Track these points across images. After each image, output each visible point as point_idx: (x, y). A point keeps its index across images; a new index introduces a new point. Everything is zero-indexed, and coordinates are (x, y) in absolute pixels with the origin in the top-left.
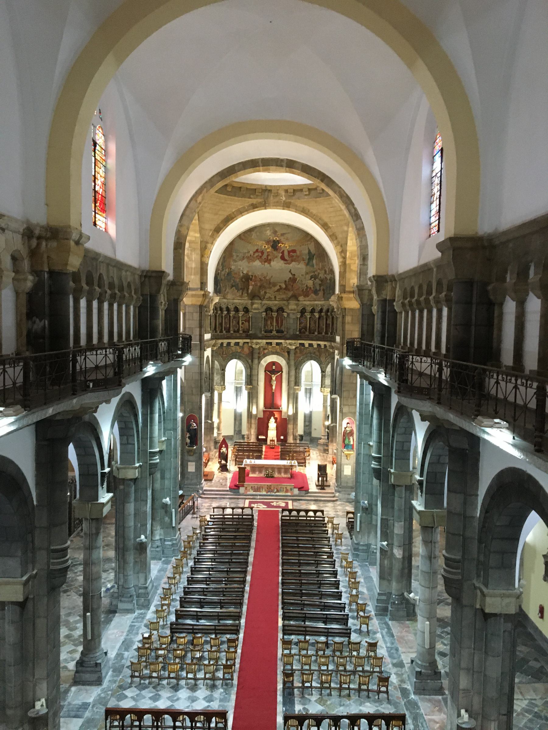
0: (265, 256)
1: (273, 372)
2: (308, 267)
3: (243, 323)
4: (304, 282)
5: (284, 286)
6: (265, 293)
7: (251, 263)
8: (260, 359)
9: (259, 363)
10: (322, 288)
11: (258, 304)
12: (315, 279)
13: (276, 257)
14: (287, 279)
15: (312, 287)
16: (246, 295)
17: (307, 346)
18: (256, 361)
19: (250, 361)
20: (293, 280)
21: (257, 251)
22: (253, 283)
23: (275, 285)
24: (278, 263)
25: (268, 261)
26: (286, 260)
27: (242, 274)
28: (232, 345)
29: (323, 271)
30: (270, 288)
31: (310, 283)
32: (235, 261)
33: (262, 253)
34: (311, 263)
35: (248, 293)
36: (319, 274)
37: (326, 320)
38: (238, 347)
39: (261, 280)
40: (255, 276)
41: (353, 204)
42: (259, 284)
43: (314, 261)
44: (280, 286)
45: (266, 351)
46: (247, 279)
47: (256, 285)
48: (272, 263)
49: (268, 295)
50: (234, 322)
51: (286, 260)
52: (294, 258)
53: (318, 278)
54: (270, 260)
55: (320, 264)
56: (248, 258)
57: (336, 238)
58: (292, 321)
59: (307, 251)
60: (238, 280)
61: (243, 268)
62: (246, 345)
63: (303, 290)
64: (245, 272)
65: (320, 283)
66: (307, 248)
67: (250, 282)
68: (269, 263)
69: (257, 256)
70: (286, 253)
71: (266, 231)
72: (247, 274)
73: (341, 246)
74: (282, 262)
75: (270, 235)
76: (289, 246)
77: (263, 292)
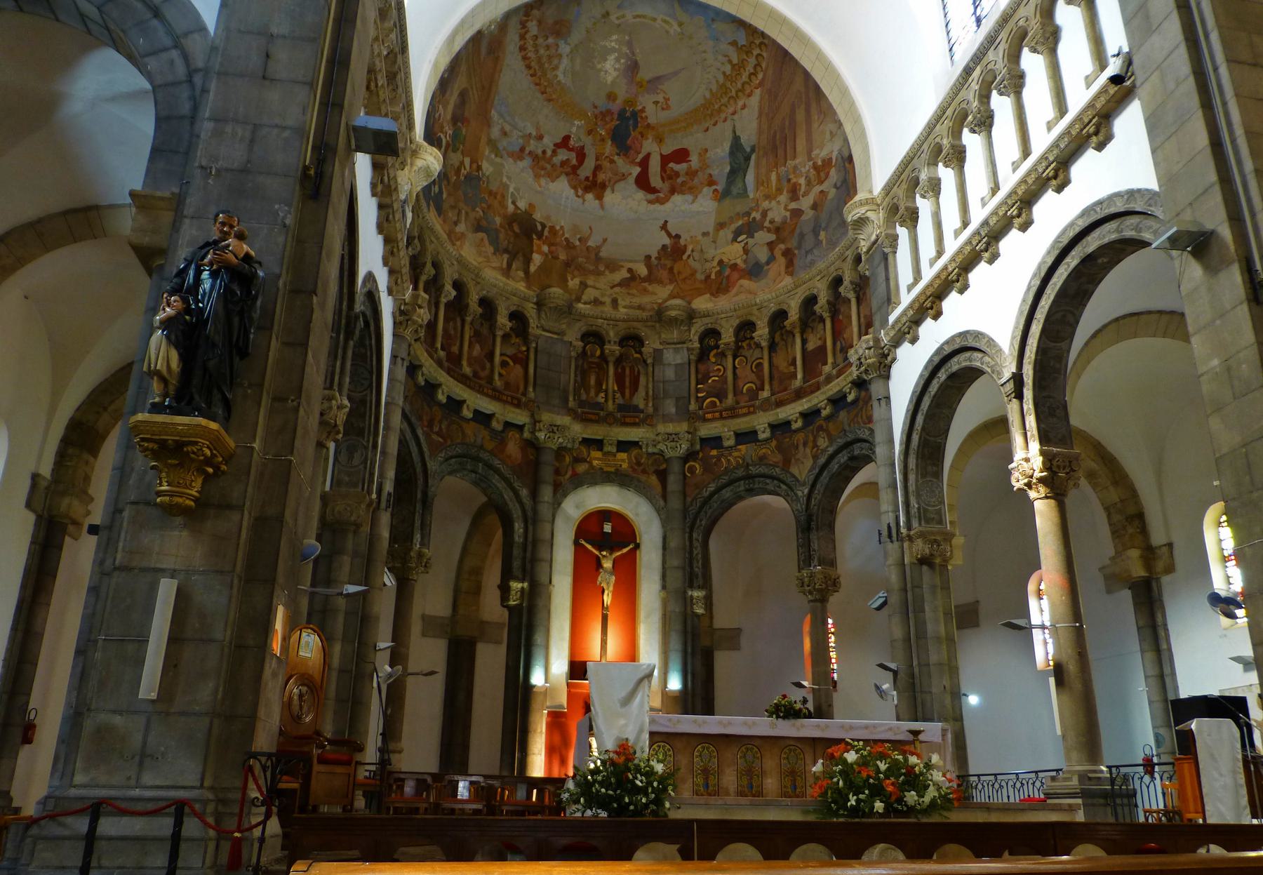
0: (586, 170)
1: (607, 543)
2: (727, 201)
3: (504, 364)
4: (711, 252)
5: (642, 270)
6: (584, 285)
7: (543, 181)
8: (560, 491)
9: (557, 504)
10: (778, 252)
13: (623, 177)
15: (739, 261)
16: (521, 274)
18: (547, 493)
19: (524, 492)
20: (675, 251)
21: (565, 143)
22: (545, 248)
23: (613, 266)
27: (511, 208)
28: (467, 413)
29: (783, 198)
30: (599, 274)
31: (733, 252)
33: (581, 156)
35: (527, 272)
36: (764, 214)
37: (804, 342)
38: (484, 433)
39: (569, 246)
40: (552, 228)
42: (563, 256)
43: (750, 178)
44: (630, 270)
45: (582, 468)
47: (556, 258)
48: (609, 197)
49: (590, 294)
50: (477, 347)
52: (679, 180)
53: (762, 228)
54: (603, 187)
55: (773, 177)
56: (536, 158)
58: (670, 374)
59: (727, 146)
60: (498, 220)
61: (517, 189)
62: (513, 435)
63: (708, 277)
64: (522, 205)
65: (772, 237)
67: (536, 242)
68: (599, 197)
69: (563, 163)
70: (655, 165)
74: (641, 195)
77: (577, 281)
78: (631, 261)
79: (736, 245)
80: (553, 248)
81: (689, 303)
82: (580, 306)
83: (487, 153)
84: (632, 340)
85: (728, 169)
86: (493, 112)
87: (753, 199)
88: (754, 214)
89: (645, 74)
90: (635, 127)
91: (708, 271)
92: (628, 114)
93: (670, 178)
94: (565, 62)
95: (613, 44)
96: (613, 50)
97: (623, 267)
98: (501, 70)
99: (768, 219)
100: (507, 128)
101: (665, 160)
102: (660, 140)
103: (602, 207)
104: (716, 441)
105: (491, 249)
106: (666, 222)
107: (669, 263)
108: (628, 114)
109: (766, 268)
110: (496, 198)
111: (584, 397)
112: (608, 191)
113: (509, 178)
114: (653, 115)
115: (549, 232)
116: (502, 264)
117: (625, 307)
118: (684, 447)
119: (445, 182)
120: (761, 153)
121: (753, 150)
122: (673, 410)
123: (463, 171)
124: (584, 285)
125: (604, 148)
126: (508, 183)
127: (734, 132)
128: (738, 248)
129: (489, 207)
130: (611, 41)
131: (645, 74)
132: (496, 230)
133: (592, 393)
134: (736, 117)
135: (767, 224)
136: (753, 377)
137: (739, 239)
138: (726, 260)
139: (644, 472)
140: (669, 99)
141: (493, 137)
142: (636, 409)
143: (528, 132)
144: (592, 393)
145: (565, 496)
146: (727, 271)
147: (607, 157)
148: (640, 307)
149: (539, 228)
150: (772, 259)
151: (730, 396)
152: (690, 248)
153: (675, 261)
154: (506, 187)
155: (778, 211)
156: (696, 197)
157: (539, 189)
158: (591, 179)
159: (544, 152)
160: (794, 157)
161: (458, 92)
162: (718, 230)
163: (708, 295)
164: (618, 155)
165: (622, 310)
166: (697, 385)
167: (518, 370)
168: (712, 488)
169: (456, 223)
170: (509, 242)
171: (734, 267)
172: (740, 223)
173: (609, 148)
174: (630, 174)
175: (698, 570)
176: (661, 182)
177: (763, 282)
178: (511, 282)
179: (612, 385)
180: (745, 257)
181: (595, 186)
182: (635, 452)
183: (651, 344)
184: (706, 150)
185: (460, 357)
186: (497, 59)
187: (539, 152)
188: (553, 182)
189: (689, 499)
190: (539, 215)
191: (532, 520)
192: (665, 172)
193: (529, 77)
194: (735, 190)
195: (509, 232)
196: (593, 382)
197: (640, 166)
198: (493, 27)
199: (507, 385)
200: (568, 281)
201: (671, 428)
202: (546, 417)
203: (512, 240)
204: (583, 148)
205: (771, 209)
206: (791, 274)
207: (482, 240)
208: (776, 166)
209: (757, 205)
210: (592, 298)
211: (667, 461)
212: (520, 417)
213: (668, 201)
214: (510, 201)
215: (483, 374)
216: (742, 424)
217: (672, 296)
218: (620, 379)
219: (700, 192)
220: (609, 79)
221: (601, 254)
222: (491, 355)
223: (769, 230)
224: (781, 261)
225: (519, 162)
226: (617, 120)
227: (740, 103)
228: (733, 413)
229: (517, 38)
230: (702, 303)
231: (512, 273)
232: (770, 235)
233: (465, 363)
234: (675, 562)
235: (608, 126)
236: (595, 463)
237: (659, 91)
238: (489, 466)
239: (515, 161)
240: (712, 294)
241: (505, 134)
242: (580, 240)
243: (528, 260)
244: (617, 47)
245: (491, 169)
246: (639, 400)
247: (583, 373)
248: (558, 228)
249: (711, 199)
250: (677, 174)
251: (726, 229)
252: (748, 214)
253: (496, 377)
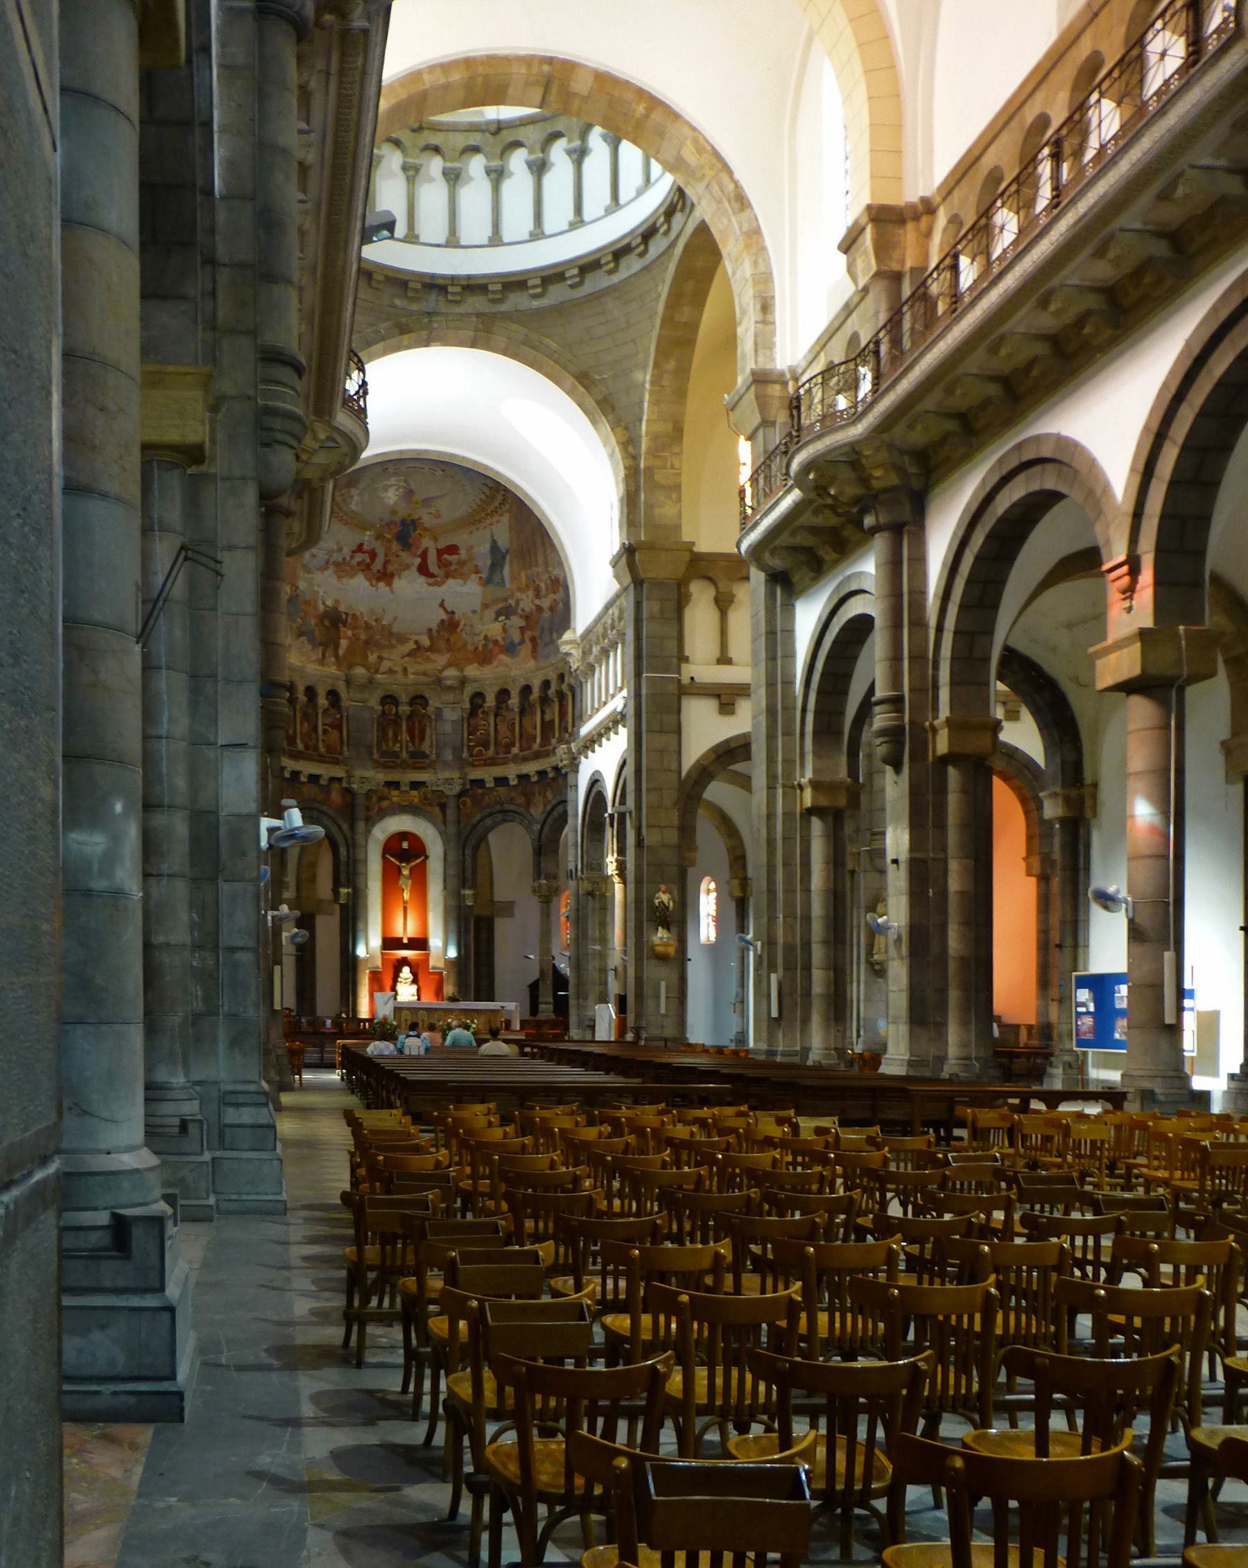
0: (378, 565)
1: (405, 856)
3: (325, 732)
5: (426, 642)
6: (381, 658)
7: (345, 580)
8: (370, 822)
9: (368, 832)
12: (508, 618)
13: (407, 567)
14: (434, 626)
15: (499, 638)
16: (333, 659)
17: (490, 784)
18: (361, 826)
19: (345, 826)
20: (450, 625)
21: (359, 549)
22: (350, 633)
23: (402, 639)
25: (385, 576)
26: (432, 576)
27: (321, 608)
29: (531, 593)
30: (392, 647)
31: (494, 629)
32: (307, 569)
33: (373, 555)
34: (496, 579)
35: (337, 656)
36: (518, 602)
37: (543, 713)
39: (368, 627)
41: (730, 172)
42: (363, 637)
43: (506, 571)
44: (416, 642)
45: (385, 804)
46: (335, 620)
47: (358, 639)
48: (397, 583)
49: (386, 665)
51: (432, 576)
52: (453, 568)
53: (515, 613)
54: (392, 575)
56: (337, 565)
57: (613, 409)
58: (448, 728)
59: (488, 546)
60: (313, 622)
62: (336, 786)
64: (329, 603)
65: (523, 623)
67: (342, 629)
68: (389, 584)
69: (359, 564)
71: (386, 488)
72: (335, 608)
73: (626, 429)
74: (422, 579)
81: (462, 670)
82: (379, 676)
84: (419, 700)
85: (489, 562)
88: (510, 601)
89: (419, 496)
94: (356, 498)
101: (440, 553)
102: (435, 539)
103: (392, 592)
104: (480, 783)
107: (446, 635)
111: (384, 748)
112: (396, 578)
114: (427, 520)
117: (414, 674)
118: (457, 789)
122: (450, 757)
124: (381, 658)
131: (419, 496)
133: (391, 743)
136: (508, 734)
139: (430, 804)
142: (424, 756)
144: (391, 743)
145: (374, 825)
146: (491, 646)
148: (424, 674)
149: (344, 616)
150: (522, 642)
151: (492, 748)
152: (462, 623)
154: (317, 593)
155: (527, 602)
165: (411, 677)
166: (469, 734)
167: (334, 734)
168: (478, 817)
171: (496, 642)
172: (500, 606)
173: (395, 546)
175: (469, 875)
178: (326, 669)
179: (405, 736)
181: (385, 576)
182: (423, 790)
183: (434, 703)
185: (295, 736)
187: (340, 559)
189: (462, 825)
191: (352, 845)
196: (391, 734)
199: (329, 748)
201: (447, 775)
202: (358, 773)
206: (535, 658)
211: (447, 796)
212: (338, 772)
215: (311, 744)
216: (498, 771)
217: (450, 665)
218: (411, 731)
222: (315, 728)
224: (528, 645)
228: (492, 762)
230: (472, 671)
233: (298, 741)
234: (451, 872)
236: (395, 799)
238: (320, 811)
240: (480, 664)
243: (337, 646)
246: (426, 747)
247: (383, 729)
250: (450, 563)
253: (321, 744)
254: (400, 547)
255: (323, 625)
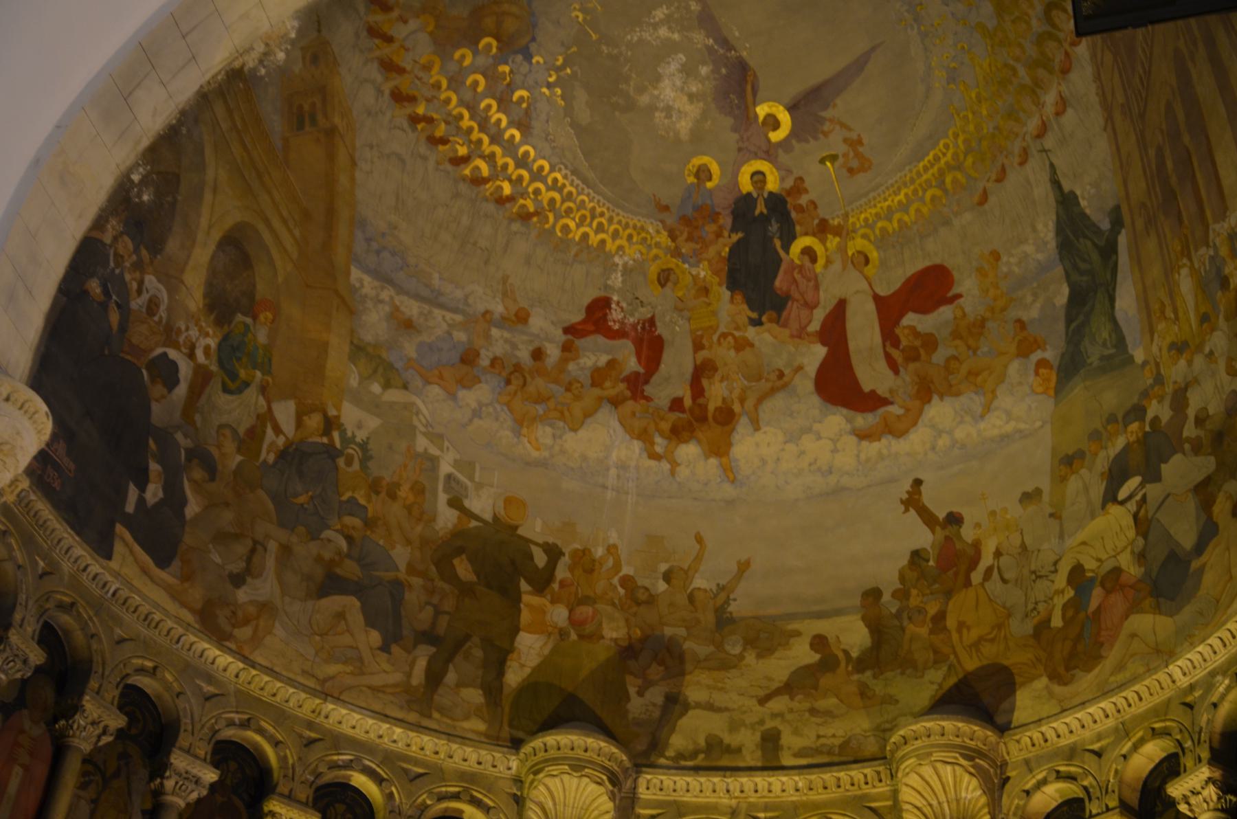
2: (1078, 391)
6: (674, 704)
7: (544, 433)
11: (578, 766)
12: (1152, 476)
13: (780, 382)
14: (887, 575)
16: (474, 696)
22: (559, 615)
24: (792, 437)
26: (871, 402)
27: (446, 518)
30: (727, 664)
35: (493, 690)
36: (1179, 400)
42: (614, 631)
43: (1126, 302)
44: (819, 642)
47: (596, 636)
51: (871, 402)
52: (939, 356)
54: (727, 417)
59: (1047, 229)
61: (466, 465)
64: (482, 504)
65: (1206, 465)
66: (1042, 191)
67: (529, 598)
68: (719, 449)
69: (598, 377)
74: (837, 420)
75: (698, 139)
76: (882, 241)
77: (656, 695)
78: (820, 615)
79: (1114, 509)
80: (585, 611)
83: (354, 382)
86: (355, 273)
87: (1145, 363)
90: (789, 237)
91: (1041, 607)
92: (761, 208)
93: (912, 356)
95: (663, 32)
96: (670, 48)
97: (798, 634)
98: (354, 163)
99: (1191, 412)
100: (412, 308)
105: (375, 637)
106: (918, 483)
108: (761, 208)
109: (1195, 564)
110: (393, 496)
112: (743, 427)
113: (436, 438)
115: (572, 568)
116: (409, 675)
119: (198, 474)
120: (1140, 224)
121: (1117, 222)
123: (269, 431)
125: (714, 313)
126: (434, 451)
127: (1056, 184)
128: (1119, 518)
129: (369, 523)
130: (656, 26)
132: (398, 587)
134: (1049, 142)
135: (1190, 430)
137: (1122, 495)
138: (1090, 564)
140: (860, 142)
141: (368, 337)
143: (481, 307)
147: (724, 336)
149: (540, 559)
153: (949, 594)
156: (995, 397)
157: (535, 454)
158: (688, 402)
159: (538, 354)
160: (1222, 214)
161: (216, 235)
162: (1063, 479)
163: (1044, 680)
164: (757, 323)
169: (238, 580)
170: (438, 612)
172: (1120, 442)
174: (800, 368)
176: (889, 373)
177: (1187, 612)
180: (1140, 542)
184: (996, 256)
186: (331, 132)
187: (524, 355)
188: (575, 430)
190: (539, 525)
192: (896, 343)
193: (449, 167)
194: (1094, 354)
195: (440, 584)
197: (824, 343)
198: (281, 56)
200: (628, 699)
203: (448, 605)
204: (652, 322)
205: (1196, 381)
207: (341, 616)
208: (1186, 252)
209: (1159, 380)
210: (702, 742)
213: (915, 423)
214: (443, 498)
219: (1002, 378)
220: (684, 127)
221: (733, 608)
223: (1197, 448)
225: (462, 393)
226: (734, 229)
227: (1050, 98)
229: (374, 72)
231: (443, 697)
232: (1199, 460)
235: (712, 251)
237: (826, 127)
239: (453, 396)
240: (1055, 677)
241: (408, 325)
242: (667, 577)
243: (499, 657)
244: (676, 36)
245: (373, 423)
248: (599, 552)
249: (1034, 392)
250: (930, 343)
251: (1084, 472)
252: (1138, 412)
254: (745, 312)
255: (451, 577)
